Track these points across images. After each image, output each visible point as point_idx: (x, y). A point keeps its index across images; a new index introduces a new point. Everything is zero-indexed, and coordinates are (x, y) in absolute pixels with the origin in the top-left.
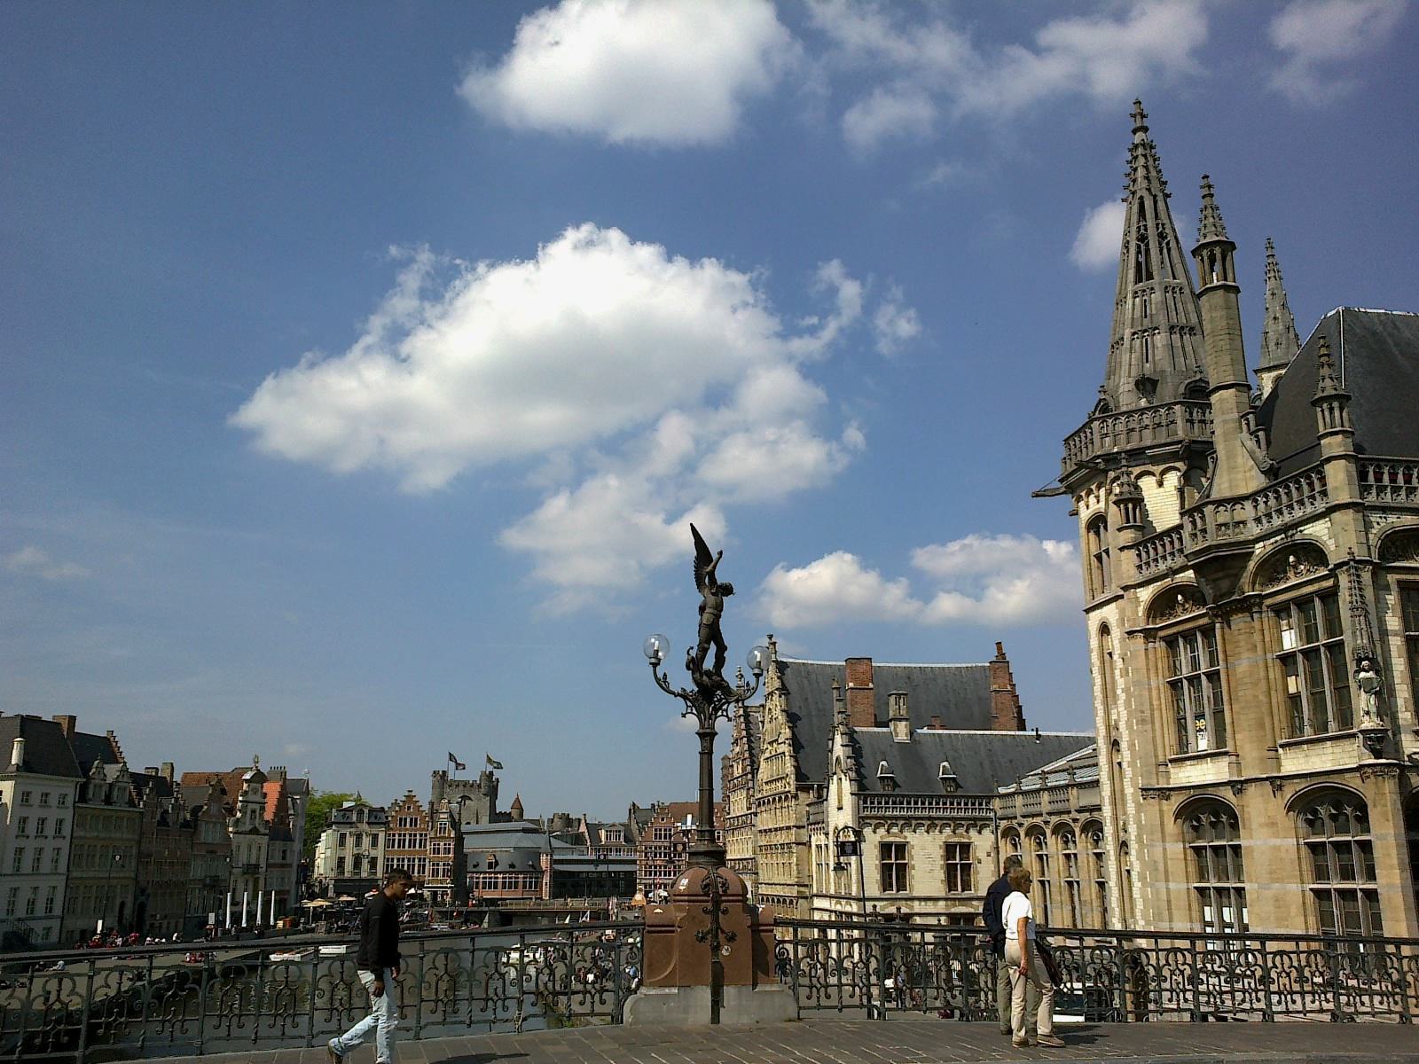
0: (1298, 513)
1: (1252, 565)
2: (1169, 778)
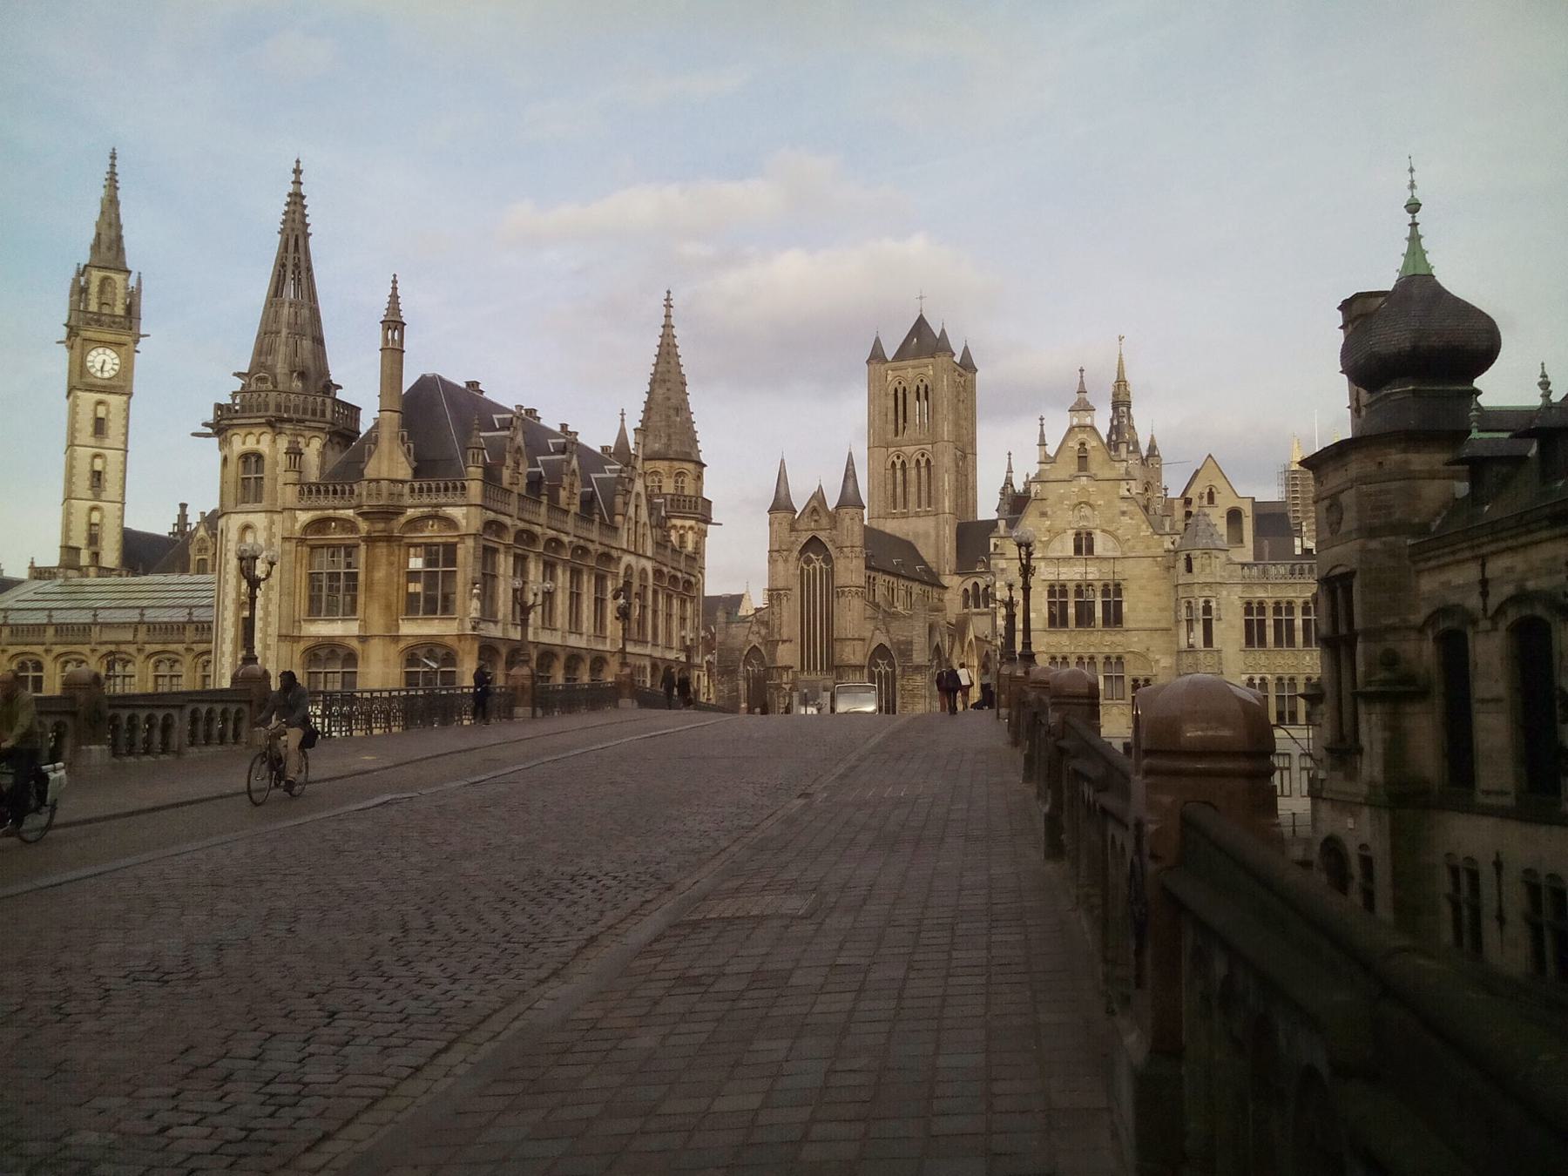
0: (442, 500)
1: (403, 519)
2: (300, 630)
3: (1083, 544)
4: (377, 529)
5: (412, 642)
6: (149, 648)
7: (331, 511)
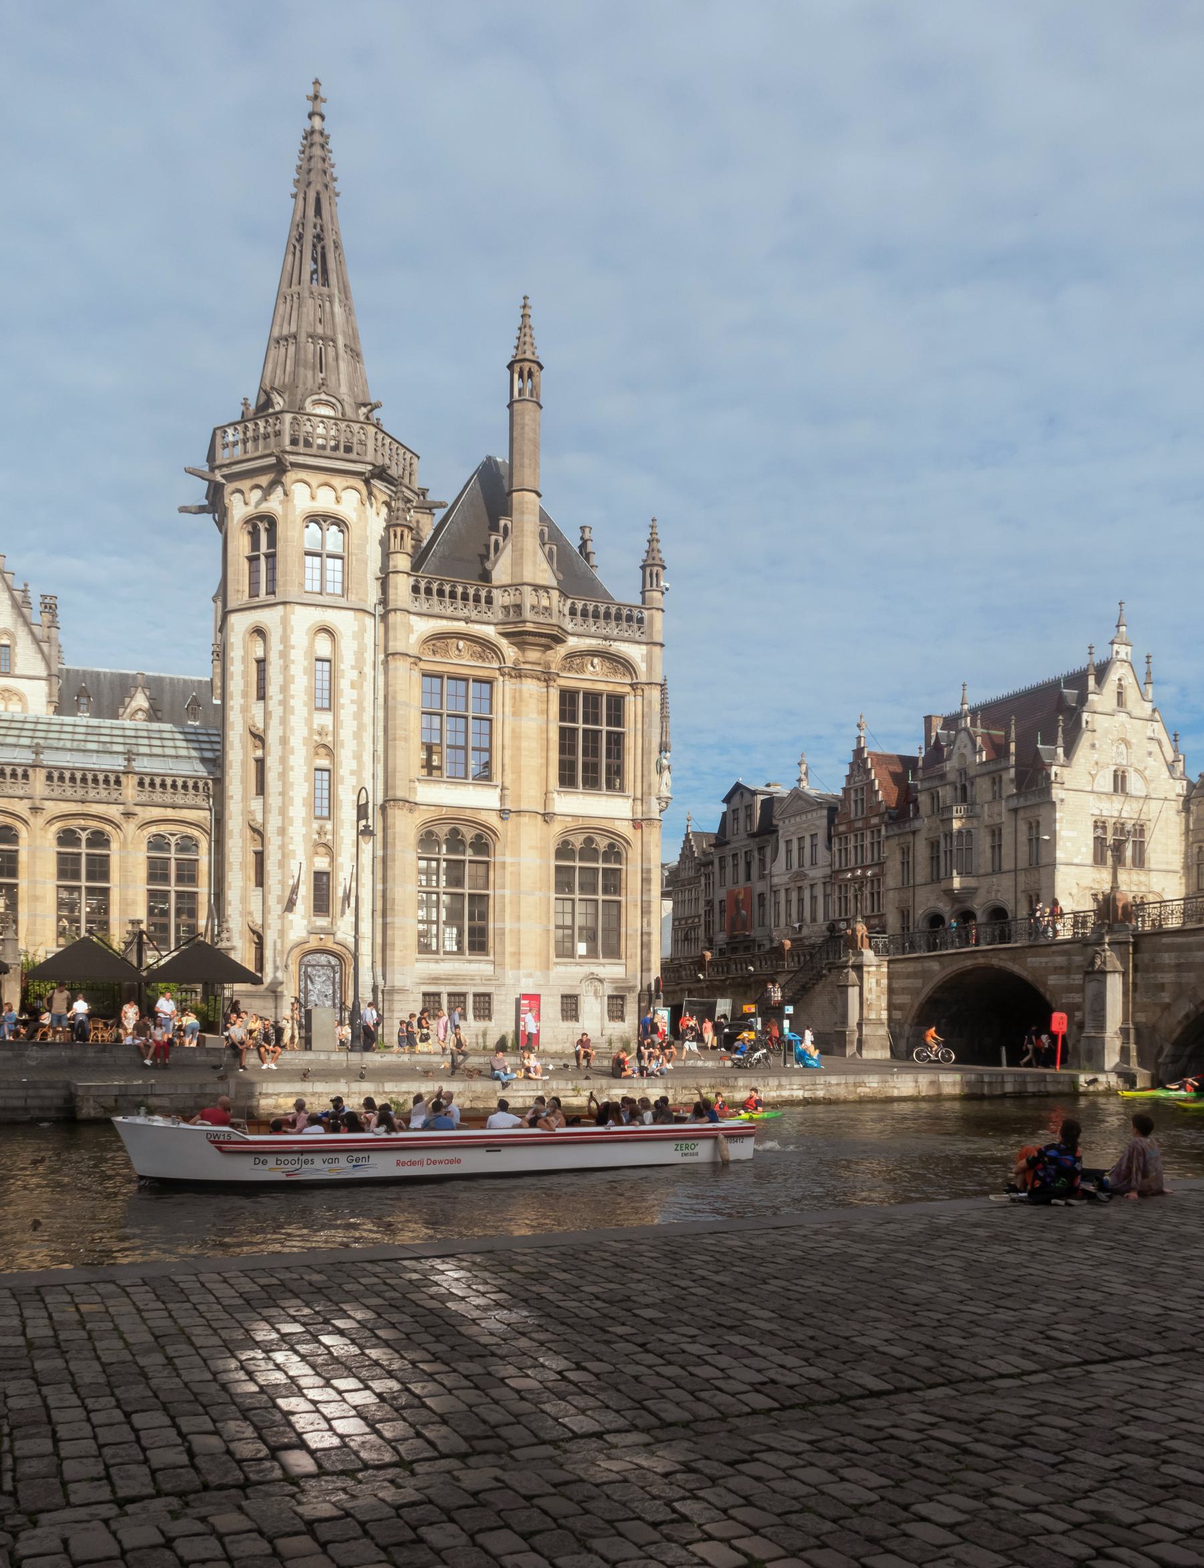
1: (561, 651)
3: (1120, 782)
4: (530, 660)
5: (572, 824)
6: (53, 808)
7: (462, 624)
